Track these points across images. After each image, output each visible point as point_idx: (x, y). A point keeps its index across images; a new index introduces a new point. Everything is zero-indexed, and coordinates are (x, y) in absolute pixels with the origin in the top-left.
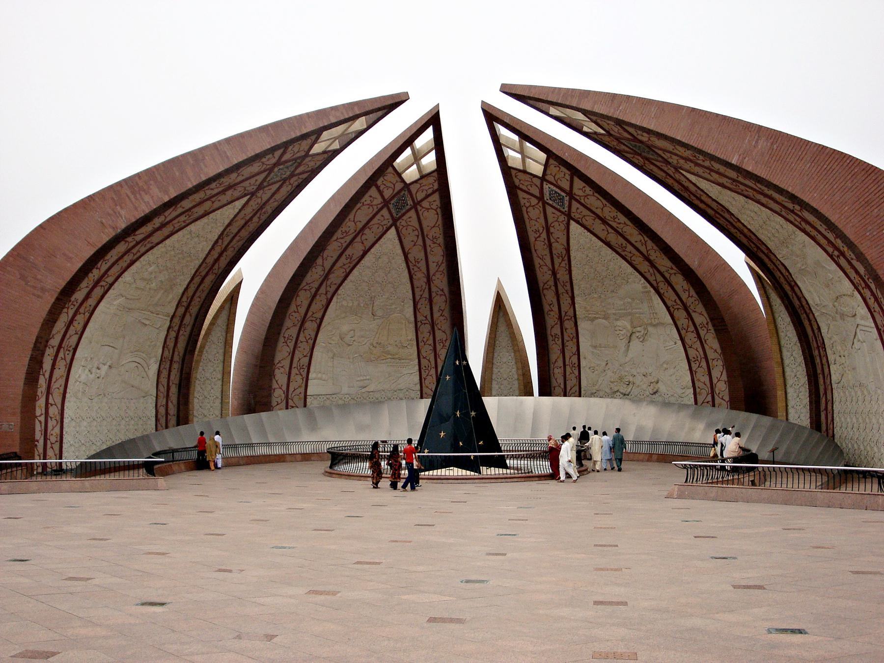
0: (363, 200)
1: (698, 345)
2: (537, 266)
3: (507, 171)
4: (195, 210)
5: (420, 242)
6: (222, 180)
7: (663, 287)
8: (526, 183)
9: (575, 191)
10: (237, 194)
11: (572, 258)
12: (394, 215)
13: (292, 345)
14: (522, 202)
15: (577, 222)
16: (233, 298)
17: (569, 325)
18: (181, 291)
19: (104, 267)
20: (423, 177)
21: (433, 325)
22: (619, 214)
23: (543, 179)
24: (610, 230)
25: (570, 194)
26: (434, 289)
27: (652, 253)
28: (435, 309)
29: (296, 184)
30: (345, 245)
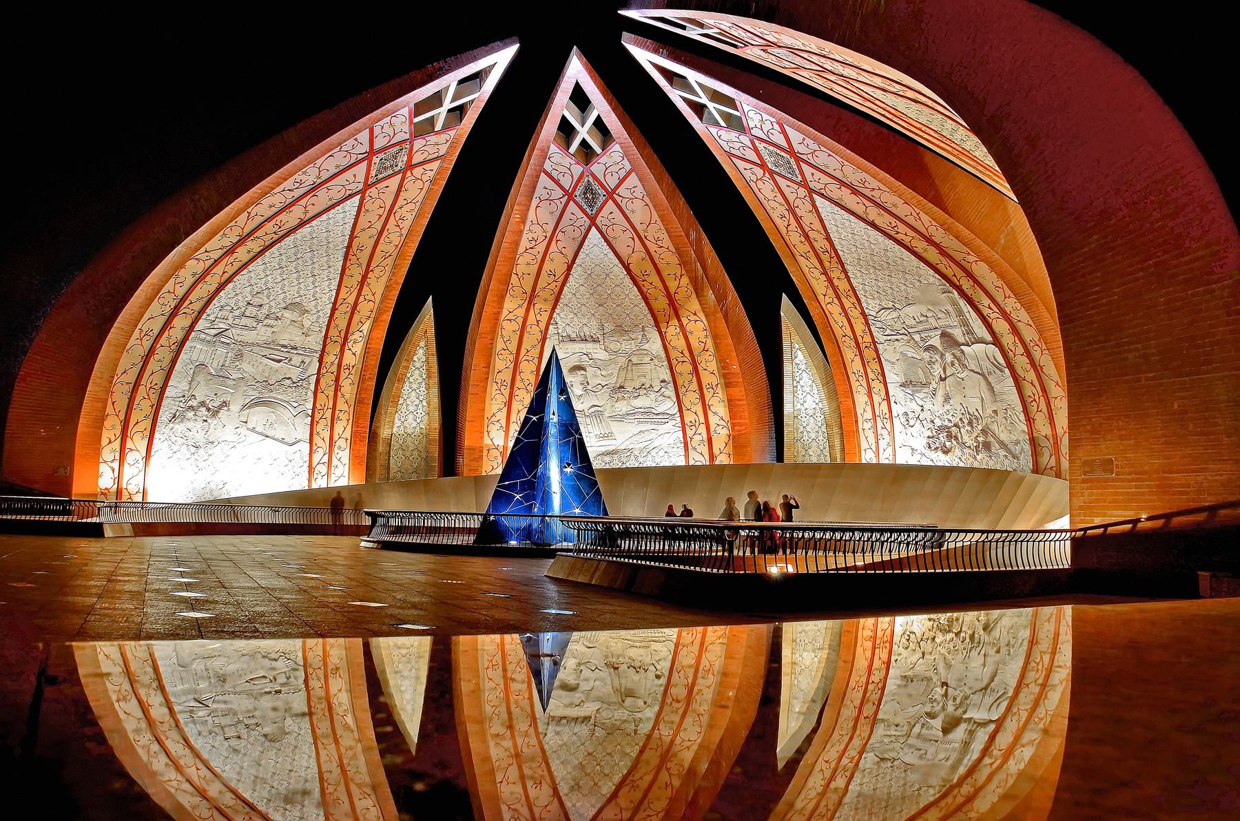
1: (1031, 376)
2: (806, 270)
4: (282, 217)
6: (297, 177)
7: (966, 284)
8: (737, 145)
9: (797, 148)
11: (841, 253)
13: (507, 392)
14: (747, 174)
15: (822, 195)
17: (869, 354)
19: (180, 292)
22: (869, 178)
24: (868, 203)
25: (791, 152)
27: (932, 230)
29: (425, 178)
30: (539, 257)
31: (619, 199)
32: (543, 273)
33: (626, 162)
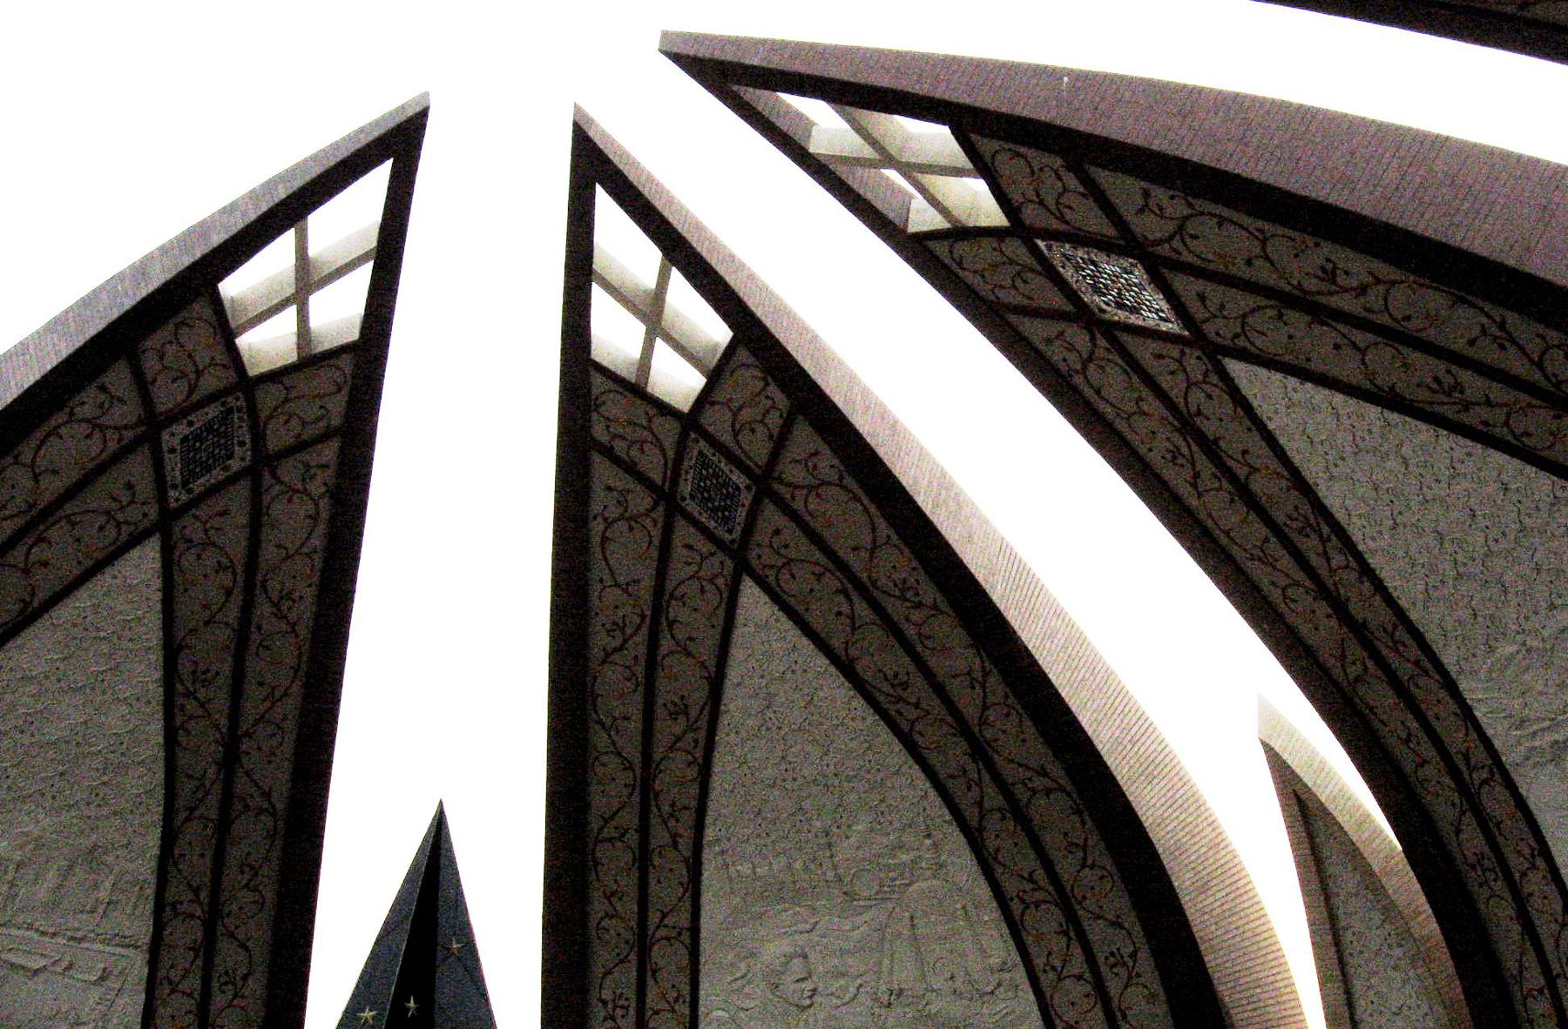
0: (596, 507)
2: (1275, 595)
3: (922, 252)
5: (863, 610)
10: (97, 538)
11: (1340, 516)
12: (727, 537)
14: (1056, 353)
15: (1243, 355)
16: (431, 898)
18: (146, 868)
20: (715, 376)
21: (1066, 902)
23: (1018, 228)
24: (1361, 338)
26: (1010, 773)
28: (1052, 840)
29: (316, 488)
30: (640, 670)
31: (785, 492)
32: (660, 712)
33: (773, 389)
